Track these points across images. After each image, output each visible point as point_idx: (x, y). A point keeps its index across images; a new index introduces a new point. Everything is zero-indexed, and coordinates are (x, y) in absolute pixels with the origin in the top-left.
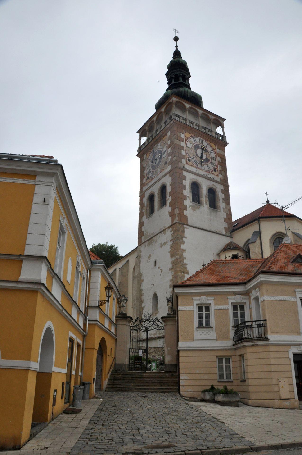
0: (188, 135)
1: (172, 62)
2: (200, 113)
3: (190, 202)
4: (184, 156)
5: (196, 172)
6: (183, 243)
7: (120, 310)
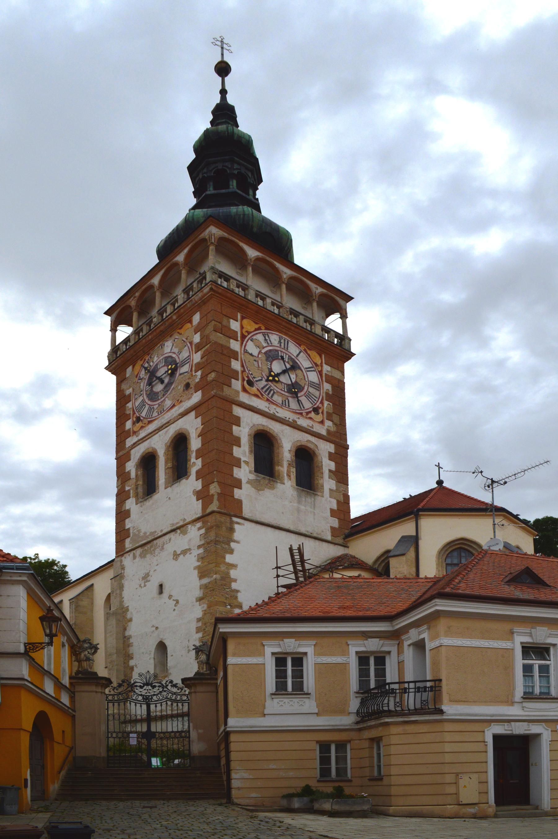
0: (250, 325)
1: (207, 132)
2: (285, 276)
3: (250, 472)
4: (237, 372)
5: (267, 410)
6: (231, 552)
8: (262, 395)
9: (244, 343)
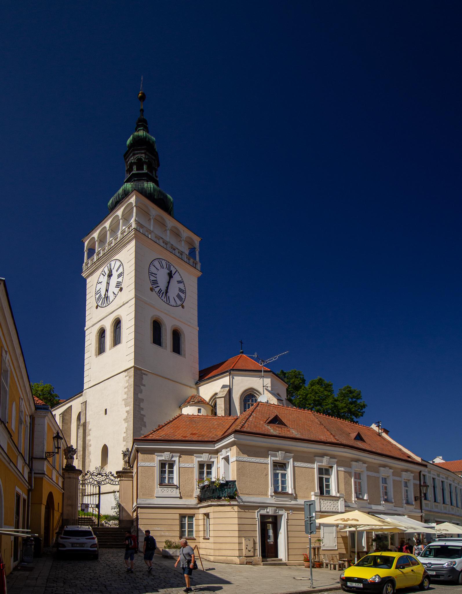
7: (67, 462)
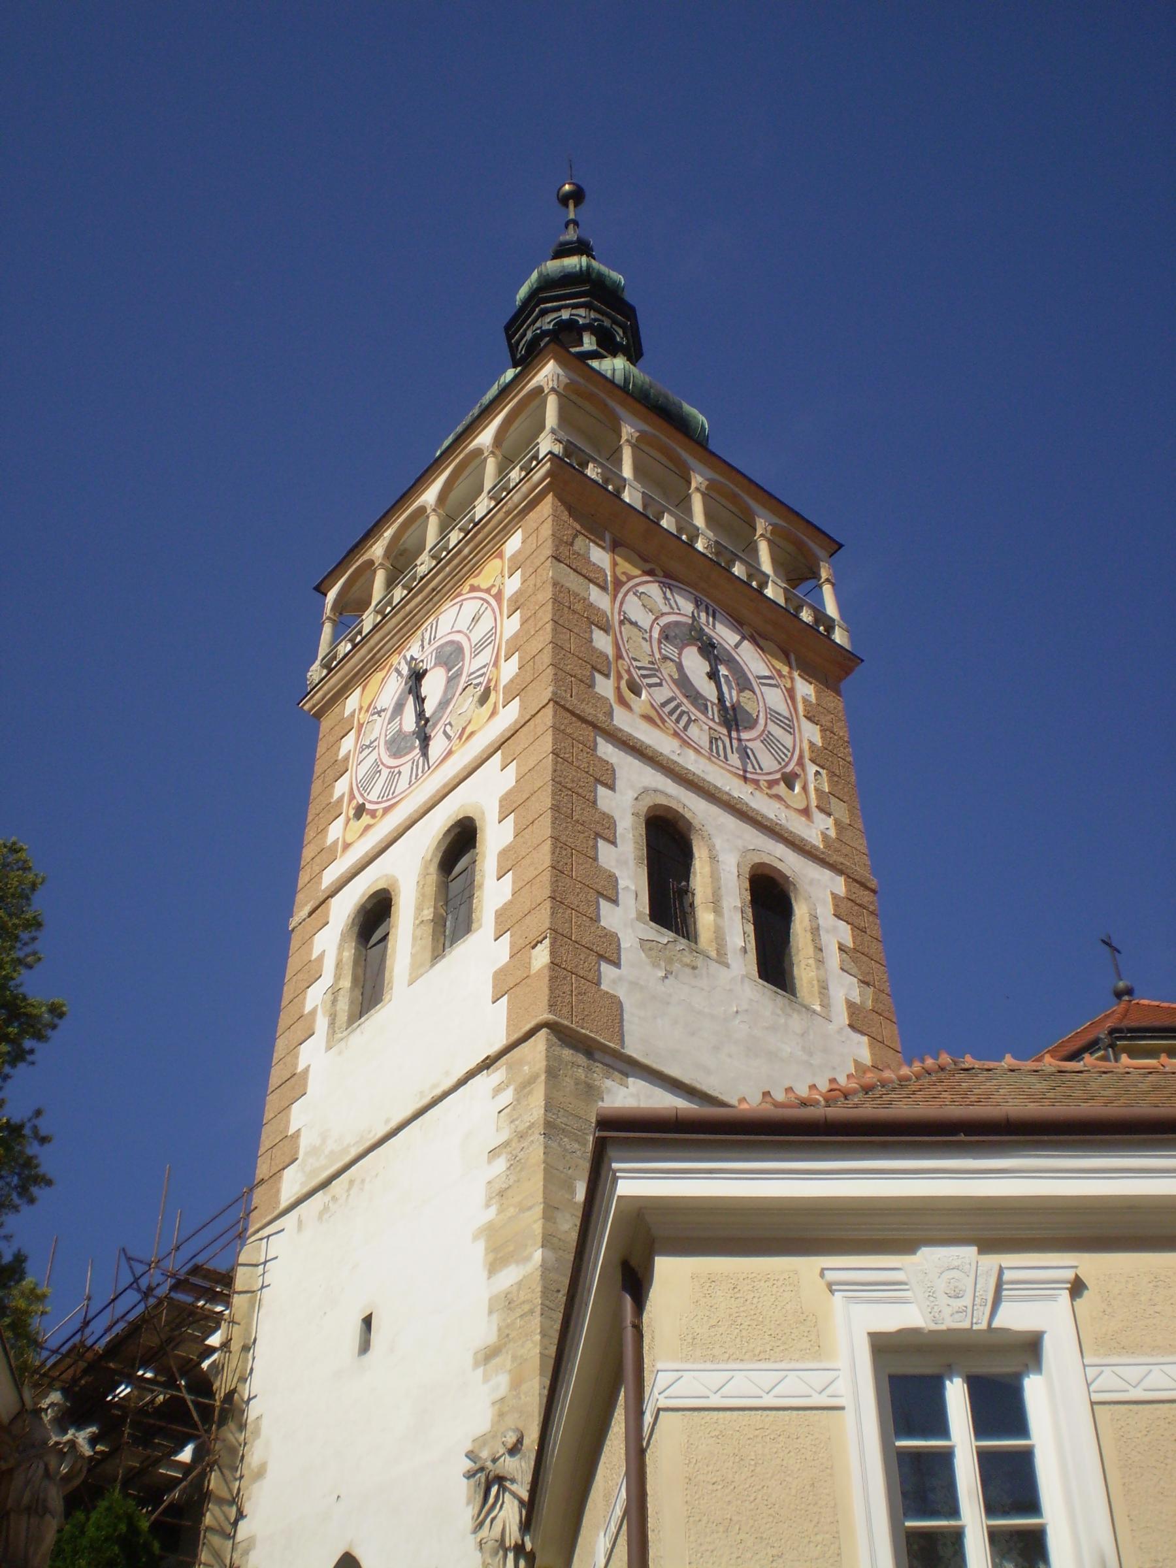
3: (639, 917)
8: (664, 721)
9: (620, 596)
